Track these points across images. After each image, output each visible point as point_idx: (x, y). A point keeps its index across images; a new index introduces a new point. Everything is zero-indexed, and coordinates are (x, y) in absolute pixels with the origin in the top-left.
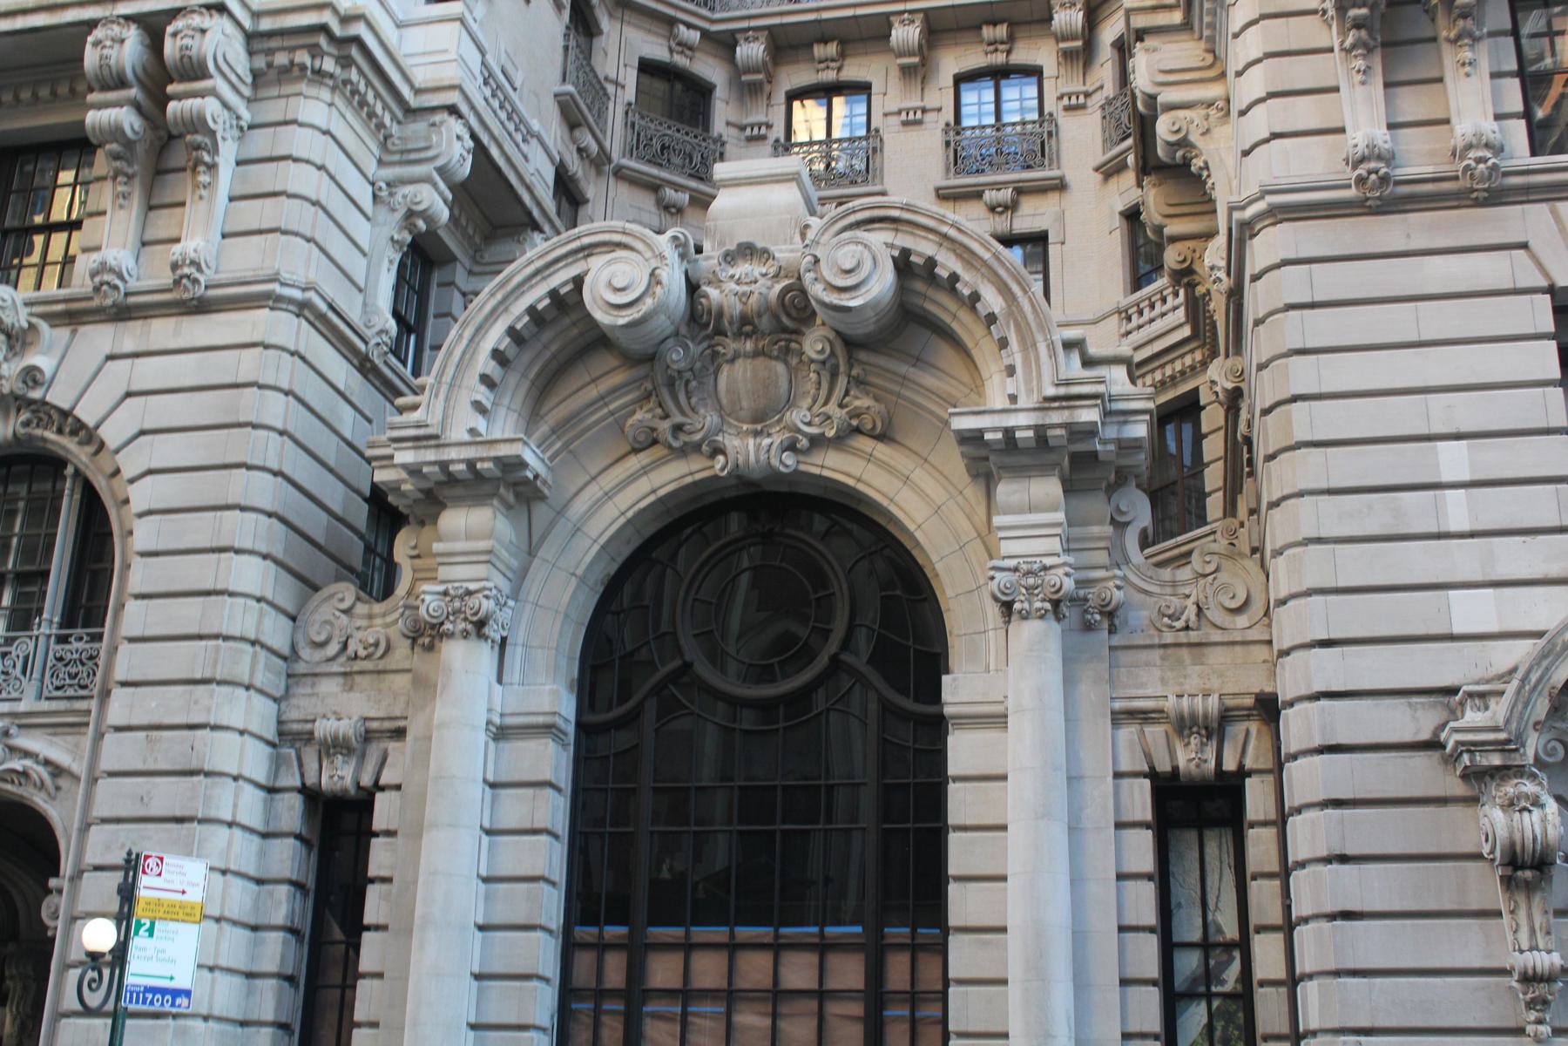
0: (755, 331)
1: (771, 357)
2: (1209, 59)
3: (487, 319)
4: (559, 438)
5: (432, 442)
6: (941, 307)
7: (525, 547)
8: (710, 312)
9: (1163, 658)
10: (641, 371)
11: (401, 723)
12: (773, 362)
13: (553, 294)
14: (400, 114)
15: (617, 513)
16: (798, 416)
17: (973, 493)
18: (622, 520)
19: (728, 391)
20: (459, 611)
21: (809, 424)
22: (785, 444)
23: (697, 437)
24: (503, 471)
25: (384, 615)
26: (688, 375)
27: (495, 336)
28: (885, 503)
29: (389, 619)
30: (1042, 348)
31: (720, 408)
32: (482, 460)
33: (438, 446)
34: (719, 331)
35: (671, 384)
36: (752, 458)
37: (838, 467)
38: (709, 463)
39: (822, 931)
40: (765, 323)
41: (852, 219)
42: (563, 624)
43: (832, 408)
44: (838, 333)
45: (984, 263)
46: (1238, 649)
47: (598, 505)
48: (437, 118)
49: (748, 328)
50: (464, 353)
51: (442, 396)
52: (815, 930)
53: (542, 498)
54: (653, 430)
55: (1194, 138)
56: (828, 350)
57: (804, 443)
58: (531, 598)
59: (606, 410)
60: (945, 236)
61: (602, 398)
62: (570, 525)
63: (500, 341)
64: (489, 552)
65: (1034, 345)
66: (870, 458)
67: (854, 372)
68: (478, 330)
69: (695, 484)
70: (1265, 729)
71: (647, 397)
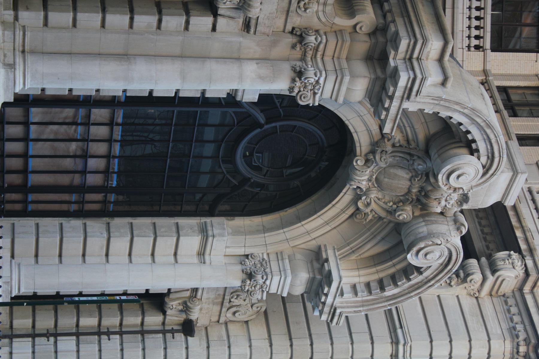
2: (499, 294)
5: (406, 96)
9: (219, 295)
10: (422, 144)
11: (252, 30)
13: (474, 141)
19: (396, 175)
20: (305, 87)
23: (378, 157)
25: (324, 11)
29: (321, 14)
30: (361, 309)
32: (387, 116)
33: (403, 97)
35: (409, 154)
37: (343, 199)
39: (114, 173)
41: (497, 154)
45: (409, 293)
46: (218, 314)
49: (423, 194)
51: (432, 101)
52: (116, 170)
55: (465, 285)
60: (429, 281)
64: (336, 100)
65: (363, 306)
66: (343, 211)
70: (182, 322)
71: (408, 141)
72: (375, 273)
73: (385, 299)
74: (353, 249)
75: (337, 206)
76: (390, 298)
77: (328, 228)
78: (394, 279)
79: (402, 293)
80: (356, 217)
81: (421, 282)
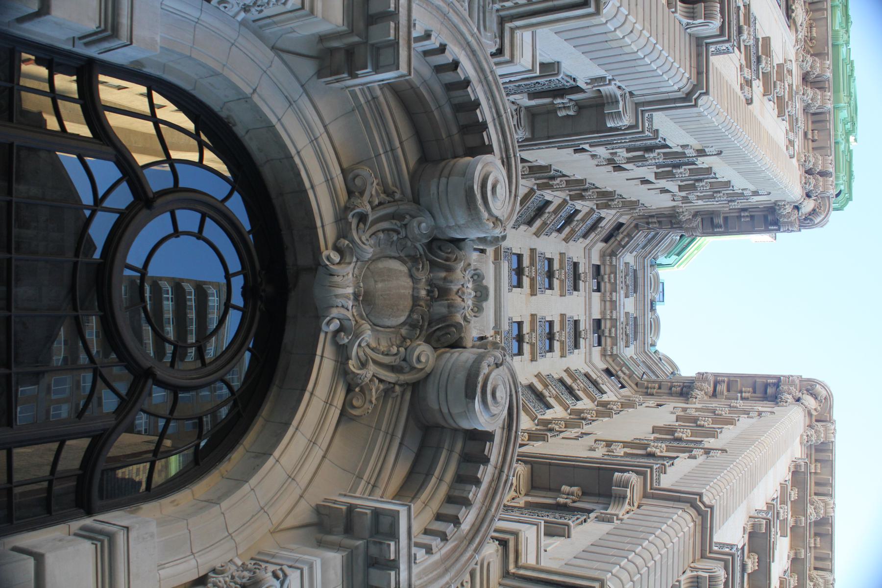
0: (433, 299)
1: (412, 311)
3: (479, 62)
4: (368, 102)
6: (446, 468)
7: (279, 44)
8: (447, 259)
12: (407, 314)
14: (502, 13)
15: (299, 147)
16: (368, 335)
17: (303, 513)
18: (293, 152)
19: (390, 270)
21: (359, 345)
22: (346, 323)
24: (373, 45)
26: (403, 233)
27: (467, 69)
28: (295, 423)
31: (374, 260)
32: (397, 29)
34: (434, 265)
36: (340, 291)
37: (323, 371)
38: (330, 245)
40: (440, 309)
42: (204, 66)
43: (372, 369)
44: (428, 375)
45: (488, 510)
47: (308, 129)
48: (498, 40)
49: (436, 293)
50: (462, 34)
53: (320, 74)
54: (362, 194)
56: (419, 366)
57: (344, 339)
58: (240, 40)
59: (381, 151)
61: (392, 150)
62: (296, 97)
63: (464, 70)
64: (312, 12)
65: (447, 570)
66: (329, 403)
67: (397, 388)
68: (473, 52)
69: (315, 228)
72: (424, 508)
73: (465, 542)
74: (372, 482)
75: (317, 393)
76: (471, 535)
77: (318, 453)
78: (466, 478)
79: (481, 516)
80: (353, 407)
81: (493, 480)
